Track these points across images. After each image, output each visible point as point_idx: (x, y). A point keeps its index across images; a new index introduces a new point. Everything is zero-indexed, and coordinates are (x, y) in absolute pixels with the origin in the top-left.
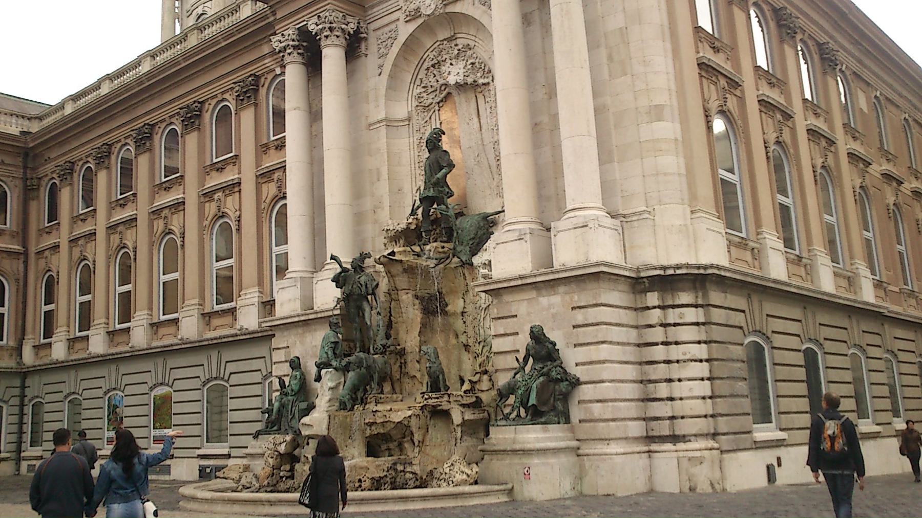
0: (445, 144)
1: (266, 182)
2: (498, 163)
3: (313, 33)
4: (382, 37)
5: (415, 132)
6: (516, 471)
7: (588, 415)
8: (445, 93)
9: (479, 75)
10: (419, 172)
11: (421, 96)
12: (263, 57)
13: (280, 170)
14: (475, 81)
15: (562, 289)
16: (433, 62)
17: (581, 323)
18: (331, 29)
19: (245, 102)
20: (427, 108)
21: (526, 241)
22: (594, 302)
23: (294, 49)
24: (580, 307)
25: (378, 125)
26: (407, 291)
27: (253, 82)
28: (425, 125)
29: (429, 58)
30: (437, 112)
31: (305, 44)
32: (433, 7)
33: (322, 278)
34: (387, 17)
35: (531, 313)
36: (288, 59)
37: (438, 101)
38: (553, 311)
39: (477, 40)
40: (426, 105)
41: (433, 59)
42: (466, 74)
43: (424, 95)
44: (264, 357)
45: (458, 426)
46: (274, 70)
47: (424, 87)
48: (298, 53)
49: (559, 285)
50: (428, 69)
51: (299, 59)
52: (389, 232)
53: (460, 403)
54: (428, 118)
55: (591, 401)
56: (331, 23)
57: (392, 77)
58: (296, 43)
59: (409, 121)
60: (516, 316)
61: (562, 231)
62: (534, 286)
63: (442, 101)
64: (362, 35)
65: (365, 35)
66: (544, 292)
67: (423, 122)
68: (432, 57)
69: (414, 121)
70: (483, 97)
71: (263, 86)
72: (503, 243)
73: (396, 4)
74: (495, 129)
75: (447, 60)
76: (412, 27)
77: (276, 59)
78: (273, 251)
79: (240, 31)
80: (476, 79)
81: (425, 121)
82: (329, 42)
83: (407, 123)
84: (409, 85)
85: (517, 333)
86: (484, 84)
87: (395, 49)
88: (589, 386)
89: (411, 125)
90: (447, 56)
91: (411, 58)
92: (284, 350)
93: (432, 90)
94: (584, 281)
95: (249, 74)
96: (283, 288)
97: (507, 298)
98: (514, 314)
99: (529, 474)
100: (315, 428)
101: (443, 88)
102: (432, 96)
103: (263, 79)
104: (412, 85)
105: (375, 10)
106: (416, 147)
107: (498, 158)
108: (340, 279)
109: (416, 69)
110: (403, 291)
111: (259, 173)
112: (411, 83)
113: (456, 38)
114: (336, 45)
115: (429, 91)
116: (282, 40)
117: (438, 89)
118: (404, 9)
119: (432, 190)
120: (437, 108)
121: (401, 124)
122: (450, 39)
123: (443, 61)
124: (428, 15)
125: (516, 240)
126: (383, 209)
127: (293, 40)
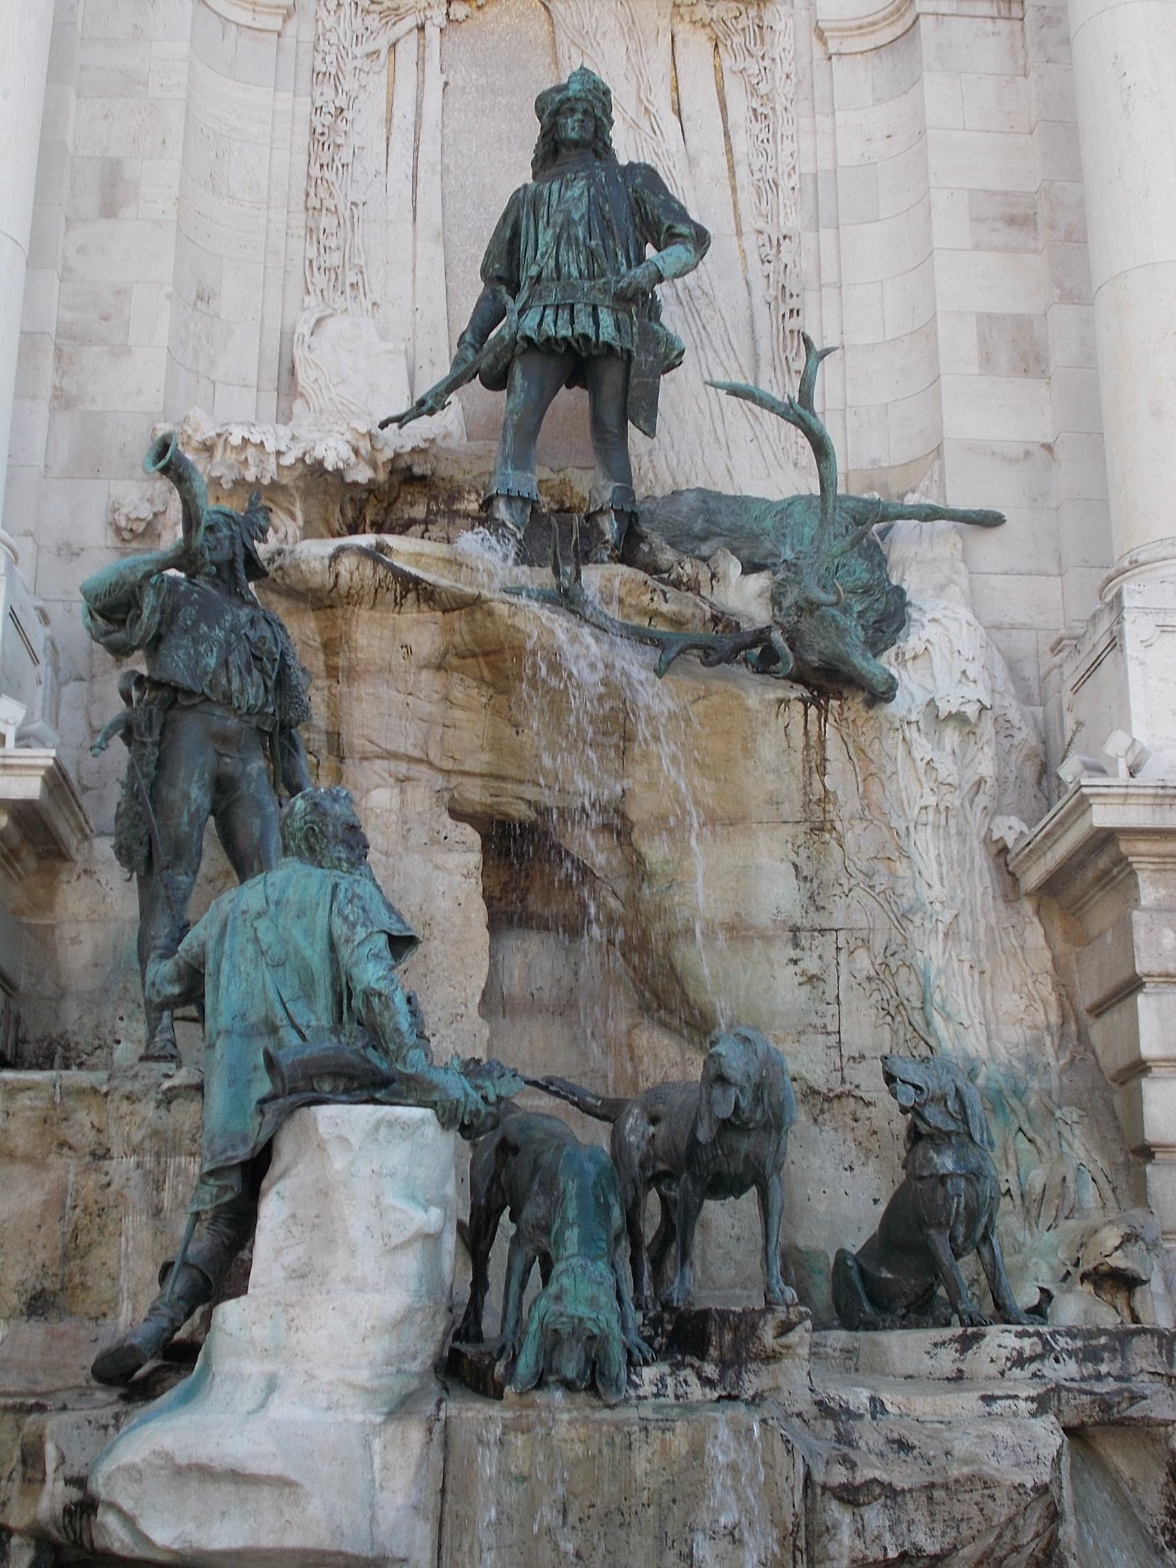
5: (306, 74)
10: (312, 252)
26: (402, 768)
28: (366, 65)
30: (432, 32)
52: (250, 452)
54: (382, 43)
59: (288, 17)
67: (359, 51)
70: (710, 46)
74: (786, 185)
83: (275, 23)
89: (288, 40)
100: (315, 1508)
106: (303, 139)
107: (794, 303)
108: (149, 600)
110: (379, 765)
119: (606, 318)
126: (120, 351)
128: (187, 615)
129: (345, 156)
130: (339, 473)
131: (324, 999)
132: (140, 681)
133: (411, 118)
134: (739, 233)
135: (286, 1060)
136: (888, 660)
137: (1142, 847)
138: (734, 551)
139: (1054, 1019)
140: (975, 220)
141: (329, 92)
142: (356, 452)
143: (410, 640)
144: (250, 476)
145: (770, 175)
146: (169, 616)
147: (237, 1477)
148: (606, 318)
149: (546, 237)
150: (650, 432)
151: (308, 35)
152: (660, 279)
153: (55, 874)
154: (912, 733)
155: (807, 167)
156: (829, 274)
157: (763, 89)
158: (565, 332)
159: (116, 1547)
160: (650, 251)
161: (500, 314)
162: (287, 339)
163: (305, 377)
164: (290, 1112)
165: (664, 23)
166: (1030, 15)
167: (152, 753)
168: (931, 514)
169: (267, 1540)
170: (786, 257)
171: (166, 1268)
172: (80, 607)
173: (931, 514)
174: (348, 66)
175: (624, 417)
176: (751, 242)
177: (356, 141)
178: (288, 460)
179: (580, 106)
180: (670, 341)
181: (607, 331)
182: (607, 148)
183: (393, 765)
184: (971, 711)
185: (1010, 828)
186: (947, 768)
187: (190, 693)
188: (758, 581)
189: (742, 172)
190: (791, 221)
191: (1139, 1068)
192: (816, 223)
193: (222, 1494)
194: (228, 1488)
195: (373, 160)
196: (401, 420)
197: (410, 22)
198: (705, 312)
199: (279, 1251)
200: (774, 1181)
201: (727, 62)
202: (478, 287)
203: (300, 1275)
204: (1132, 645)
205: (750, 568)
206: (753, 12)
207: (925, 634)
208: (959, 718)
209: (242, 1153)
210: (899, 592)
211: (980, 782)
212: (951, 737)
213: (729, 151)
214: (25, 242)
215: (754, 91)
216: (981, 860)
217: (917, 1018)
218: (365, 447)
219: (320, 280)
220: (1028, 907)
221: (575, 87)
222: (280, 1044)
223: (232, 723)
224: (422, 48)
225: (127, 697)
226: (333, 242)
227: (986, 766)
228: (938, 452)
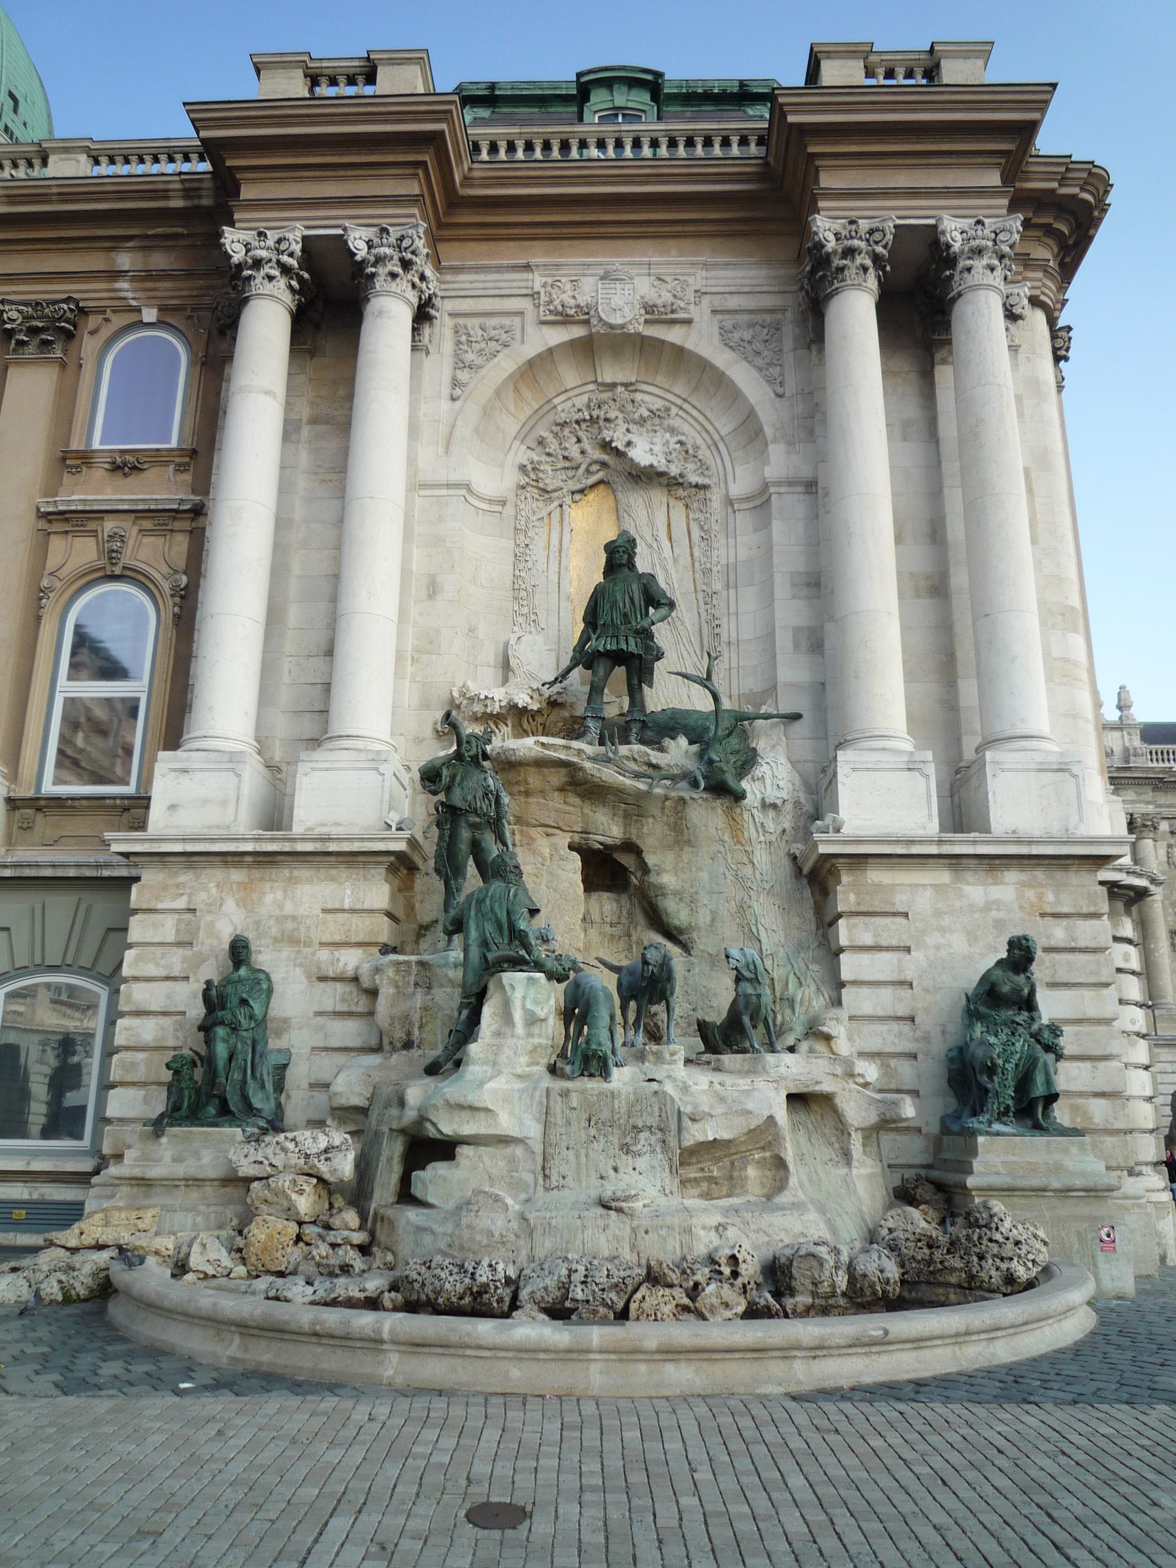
0: (643, 564)
1: (66, 532)
2: (717, 631)
3: (358, 258)
4: (472, 333)
5: (512, 529)
6: (1079, 1233)
7: (1079, 1120)
8: (593, 479)
9: (691, 466)
10: (516, 608)
11: (542, 468)
12: (115, 275)
13: (123, 516)
14: (681, 475)
15: (1012, 876)
16: (579, 416)
17: (1062, 945)
18: (406, 265)
19: (31, 348)
20: (547, 496)
21: (927, 777)
22: (1092, 909)
23: (281, 273)
24: (1056, 915)
25: (444, 492)
27: (69, 314)
28: (537, 524)
29: (569, 403)
31: (306, 276)
32: (629, 315)
33: (328, 765)
34: (490, 300)
35: (944, 913)
36: (259, 285)
37: (575, 488)
38: (994, 914)
39: (686, 406)
40: (549, 489)
41: (579, 410)
42: (669, 458)
43: (548, 468)
44: (7, 929)
45: (857, 1130)
46: (140, 311)
47: (549, 454)
48: (290, 287)
49: (1008, 867)
50: (564, 424)
51: (287, 297)
52: (489, 702)
53: (861, 1080)
54: (544, 513)
55: (1081, 1094)
56: (413, 253)
57: (487, 412)
58: (294, 263)
60: (906, 915)
61: (1009, 770)
62: (954, 861)
63: (581, 491)
64: (433, 312)
65: (437, 315)
66: (969, 876)
67: (534, 518)
68: (579, 406)
69: (509, 510)
70: (684, 508)
71: (92, 333)
72: (868, 769)
73: (523, 284)
74: (715, 569)
75: (620, 421)
76: (557, 336)
77: (155, 290)
78: (58, 689)
79: (65, 197)
80: (685, 472)
81: (540, 516)
82: (394, 286)
83: (498, 508)
84: (510, 440)
85: (908, 950)
86: (697, 486)
87: (507, 364)
88: (1081, 1064)
90: (620, 416)
91: (527, 393)
92: (177, 916)
93: (568, 464)
94: (1066, 867)
95: (65, 296)
96: (185, 771)
97: (876, 876)
98: (901, 908)
99: (1114, 1241)
101: (595, 468)
102: (562, 475)
103: (93, 321)
104: (517, 443)
105: (462, 277)
107: (717, 622)
108: (445, 772)
109: (530, 417)
111: (51, 509)
112: (515, 438)
113: (636, 390)
114: (408, 302)
115: (559, 466)
116: (255, 243)
117: (583, 467)
118: (543, 298)
119: (632, 641)
120: (568, 500)
121: (486, 506)
122: (626, 385)
123: (607, 420)
124: (612, 327)
125: (902, 770)
127: (291, 255)
128: (458, 778)
129: (530, 565)
130: (525, 708)
131: (506, 933)
132: (442, 803)
133: (557, 546)
134: (696, 591)
135: (490, 956)
136: (745, 784)
137: (842, 860)
138: (686, 735)
139: (814, 927)
140: (793, 585)
141: (522, 537)
142: (532, 698)
143: (550, 779)
144: (489, 711)
145: (708, 566)
146: (453, 777)
147: (472, 1108)
148: (632, 641)
149: (607, 607)
150: (651, 687)
151: (513, 513)
152: (653, 624)
153: (413, 875)
154: (755, 812)
155: (724, 562)
156: (733, 609)
157: (706, 527)
158: (614, 648)
159: (431, 1135)
160: (652, 611)
161: (589, 639)
162: (506, 645)
163: (513, 662)
164: (493, 974)
165: (665, 500)
166: (820, 492)
167: (447, 833)
168: (767, 717)
169: (483, 1131)
170: (715, 602)
171: (451, 1031)
172: (417, 776)
173: (767, 717)
174: (530, 526)
175: (640, 682)
176: (700, 596)
177: (534, 558)
178: (503, 704)
179: (621, 549)
180: (658, 648)
181: (632, 648)
182: (634, 566)
183: (545, 829)
184: (779, 802)
185: (798, 848)
186: (771, 826)
187: (461, 810)
188: (695, 748)
189: (697, 564)
190: (718, 586)
191: (841, 950)
192: (728, 586)
193: (465, 1115)
194: (469, 1113)
195: (541, 566)
196: (552, 684)
197: (556, 503)
198: (680, 628)
199: (489, 1026)
200: (671, 999)
201: (691, 516)
202: (582, 626)
203: (498, 1034)
204: (840, 777)
205: (691, 743)
206: (702, 492)
207: (762, 769)
208: (774, 806)
209: (476, 990)
210: (754, 750)
211: (784, 831)
212: (771, 813)
213: (692, 555)
214: (396, 619)
215: (702, 528)
216: (786, 862)
217: (754, 930)
218: (536, 696)
219: (520, 620)
220: (805, 881)
221: (620, 541)
222: (489, 950)
223: (478, 820)
224: (562, 514)
225: (437, 809)
226: (525, 603)
227: (787, 825)
228: (775, 687)
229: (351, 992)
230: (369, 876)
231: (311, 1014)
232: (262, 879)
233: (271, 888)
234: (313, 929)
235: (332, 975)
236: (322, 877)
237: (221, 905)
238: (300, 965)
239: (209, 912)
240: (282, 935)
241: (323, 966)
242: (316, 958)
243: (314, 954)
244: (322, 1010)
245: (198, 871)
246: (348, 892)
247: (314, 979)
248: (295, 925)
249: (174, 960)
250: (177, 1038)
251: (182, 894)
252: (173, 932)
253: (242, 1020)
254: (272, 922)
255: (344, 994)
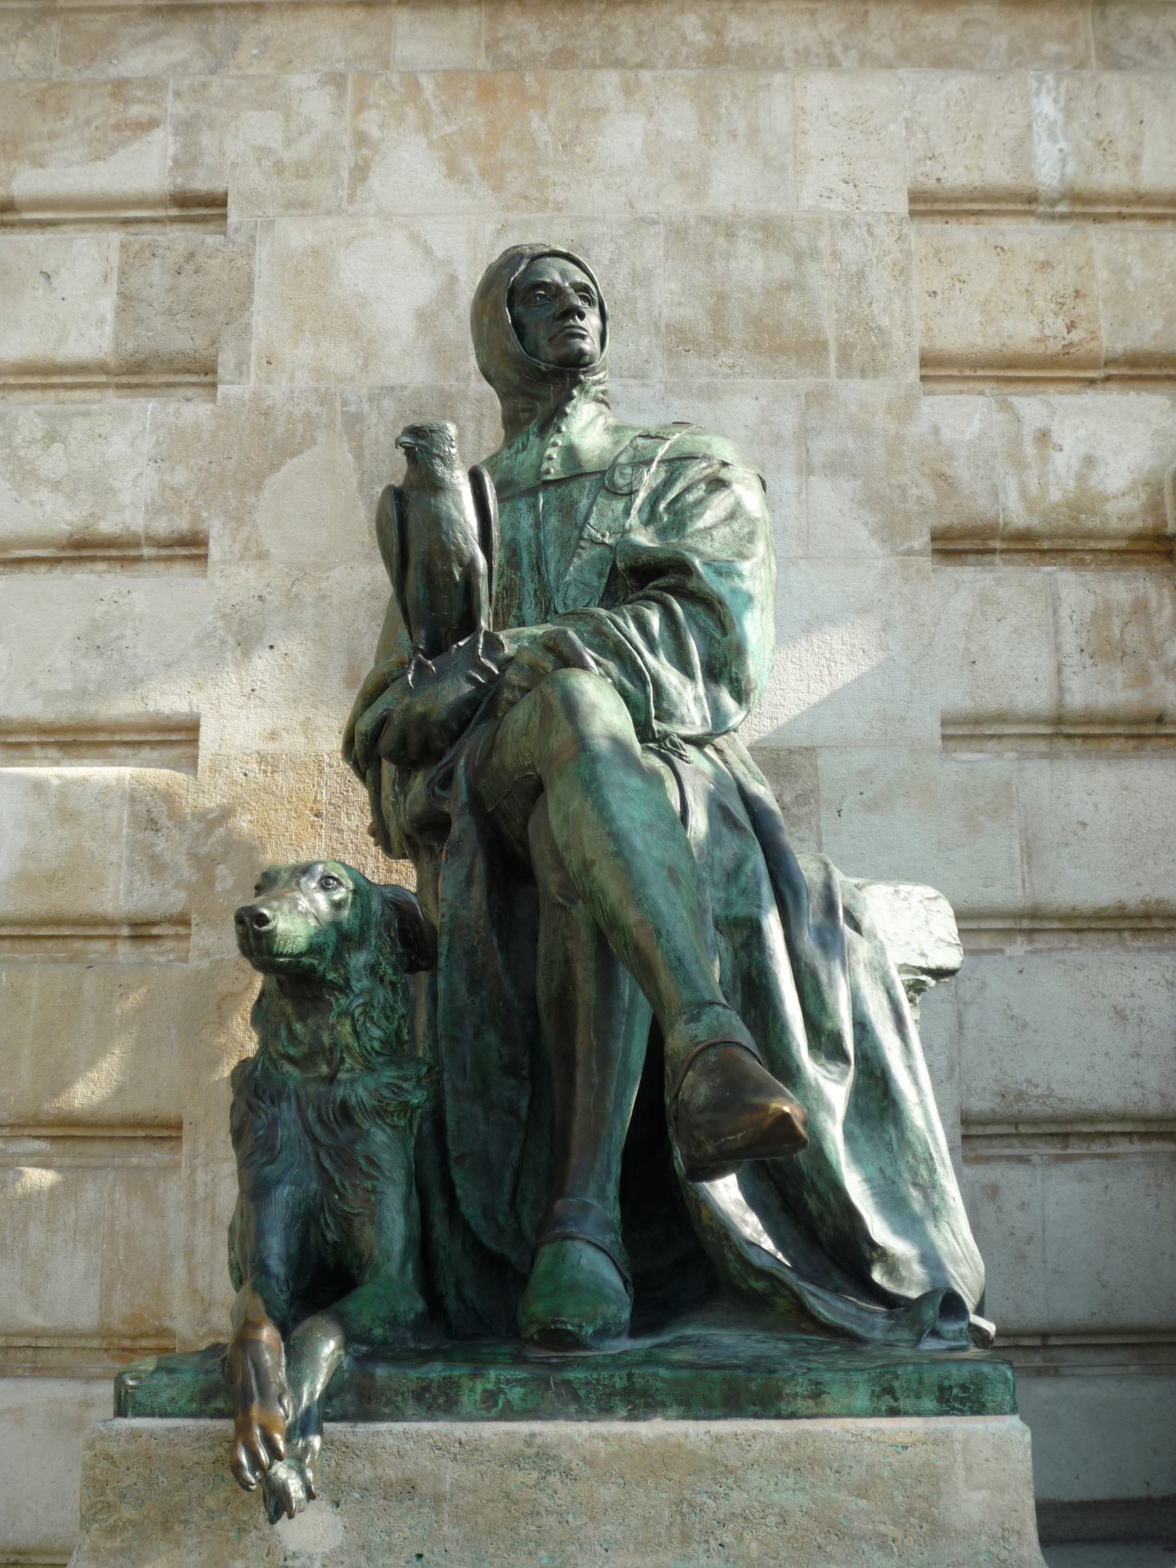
92: (116, 236)
229: (1141, 608)
230: (1128, 47)
231: (932, 729)
232: (563, 59)
233: (628, 90)
234: (880, 282)
235: (1017, 515)
236: (886, 49)
237: (361, 172)
238: (836, 466)
239: (300, 206)
240: (717, 315)
241: (963, 472)
242: (918, 429)
243: (904, 410)
244: (990, 702)
245: (219, 27)
246: (1047, 106)
247: (921, 541)
248: (783, 265)
249: (118, 446)
250: (157, 867)
251: (148, 125)
252: (107, 305)
253: (670, 676)
254: (652, 249)
255: (1102, 615)
